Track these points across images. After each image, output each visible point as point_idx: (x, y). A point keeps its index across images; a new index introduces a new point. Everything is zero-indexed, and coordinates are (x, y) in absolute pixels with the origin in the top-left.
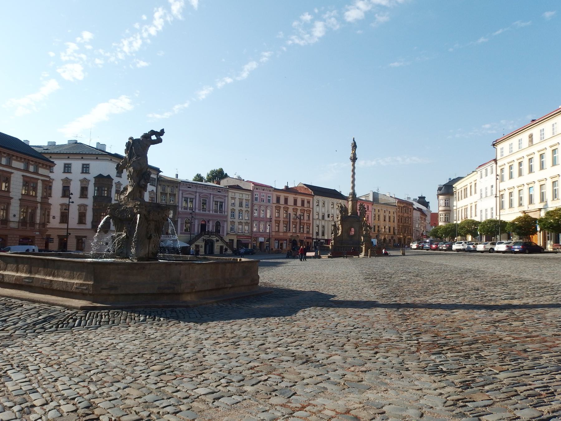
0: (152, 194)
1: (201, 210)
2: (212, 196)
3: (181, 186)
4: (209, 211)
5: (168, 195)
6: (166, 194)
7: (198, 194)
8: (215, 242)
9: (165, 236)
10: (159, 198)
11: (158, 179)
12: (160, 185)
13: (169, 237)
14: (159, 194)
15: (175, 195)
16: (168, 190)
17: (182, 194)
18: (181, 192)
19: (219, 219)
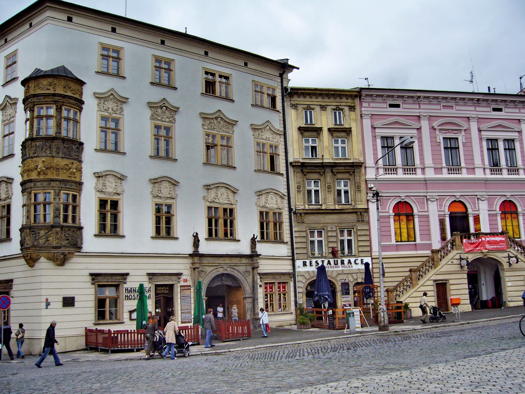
0: (267, 134)
1: (445, 171)
2: (474, 126)
3: (364, 105)
4: (472, 170)
5: (325, 133)
6: (318, 131)
7: (425, 124)
8: (506, 266)
9: (329, 263)
10: (296, 146)
11: (284, 90)
12: (295, 106)
13: (342, 262)
14: (293, 134)
15: (348, 131)
16: (324, 118)
17: (373, 128)
18: (367, 123)
19: (509, 195)
